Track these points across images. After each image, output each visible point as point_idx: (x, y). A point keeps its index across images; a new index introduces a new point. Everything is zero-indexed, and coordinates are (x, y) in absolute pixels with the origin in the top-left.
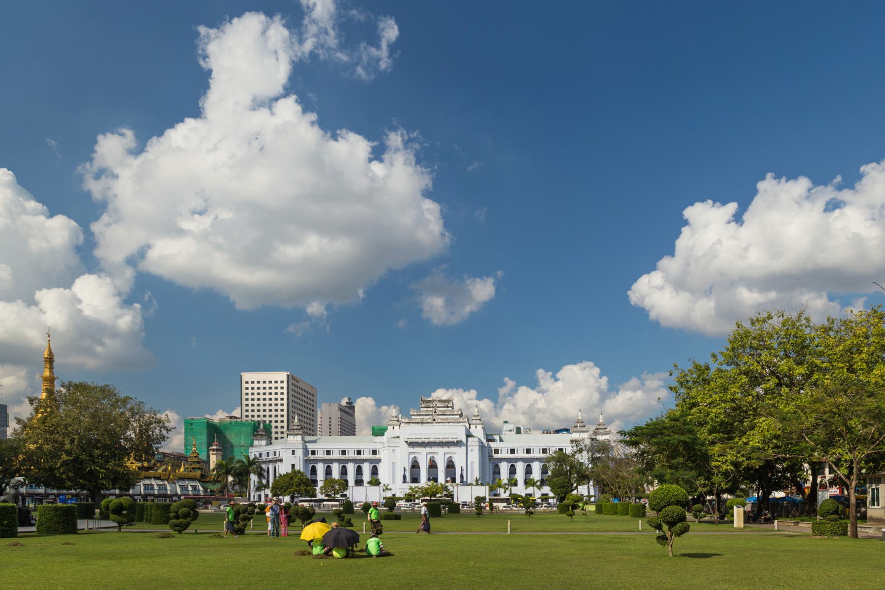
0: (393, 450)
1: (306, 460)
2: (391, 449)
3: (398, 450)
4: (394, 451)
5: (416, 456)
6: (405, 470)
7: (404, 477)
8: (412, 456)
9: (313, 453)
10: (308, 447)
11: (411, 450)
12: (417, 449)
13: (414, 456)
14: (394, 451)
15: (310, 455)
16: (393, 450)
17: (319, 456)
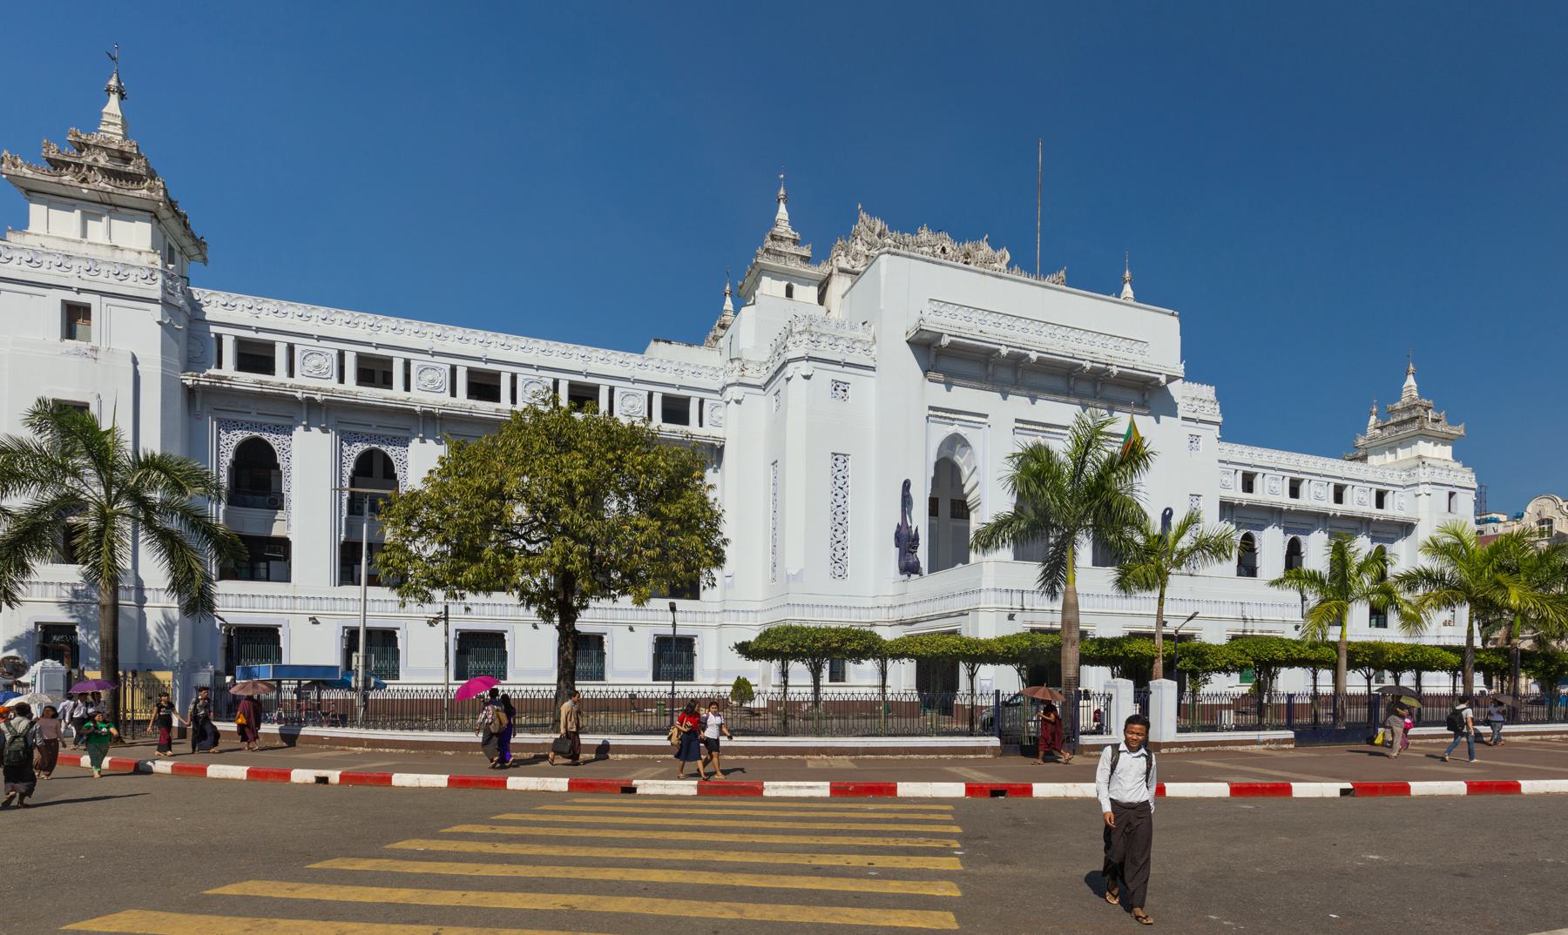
0: (836, 384)
1: (191, 393)
2: (825, 375)
3: (862, 385)
4: (839, 388)
5: (962, 431)
6: (906, 501)
7: (905, 541)
8: (942, 431)
9: (255, 356)
10: (211, 313)
11: (938, 394)
12: (965, 397)
13: (951, 430)
14: (839, 388)
15: (229, 367)
16: (836, 384)
17: (298, 379)
